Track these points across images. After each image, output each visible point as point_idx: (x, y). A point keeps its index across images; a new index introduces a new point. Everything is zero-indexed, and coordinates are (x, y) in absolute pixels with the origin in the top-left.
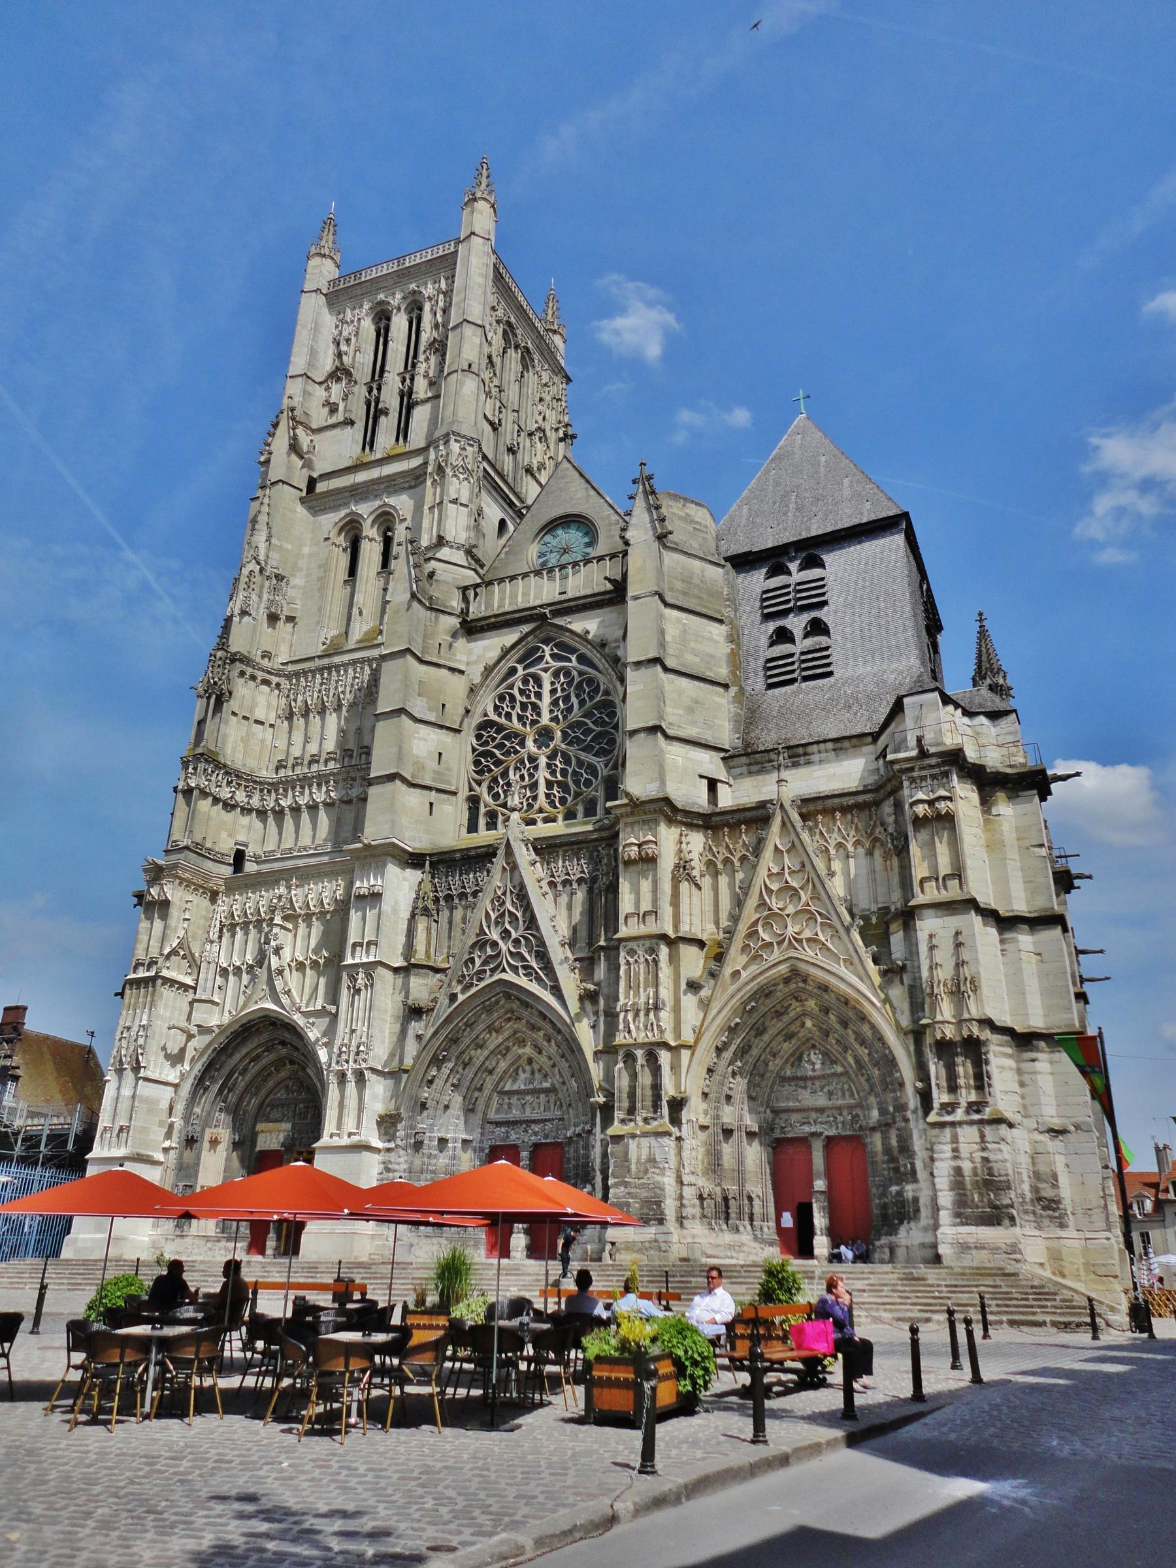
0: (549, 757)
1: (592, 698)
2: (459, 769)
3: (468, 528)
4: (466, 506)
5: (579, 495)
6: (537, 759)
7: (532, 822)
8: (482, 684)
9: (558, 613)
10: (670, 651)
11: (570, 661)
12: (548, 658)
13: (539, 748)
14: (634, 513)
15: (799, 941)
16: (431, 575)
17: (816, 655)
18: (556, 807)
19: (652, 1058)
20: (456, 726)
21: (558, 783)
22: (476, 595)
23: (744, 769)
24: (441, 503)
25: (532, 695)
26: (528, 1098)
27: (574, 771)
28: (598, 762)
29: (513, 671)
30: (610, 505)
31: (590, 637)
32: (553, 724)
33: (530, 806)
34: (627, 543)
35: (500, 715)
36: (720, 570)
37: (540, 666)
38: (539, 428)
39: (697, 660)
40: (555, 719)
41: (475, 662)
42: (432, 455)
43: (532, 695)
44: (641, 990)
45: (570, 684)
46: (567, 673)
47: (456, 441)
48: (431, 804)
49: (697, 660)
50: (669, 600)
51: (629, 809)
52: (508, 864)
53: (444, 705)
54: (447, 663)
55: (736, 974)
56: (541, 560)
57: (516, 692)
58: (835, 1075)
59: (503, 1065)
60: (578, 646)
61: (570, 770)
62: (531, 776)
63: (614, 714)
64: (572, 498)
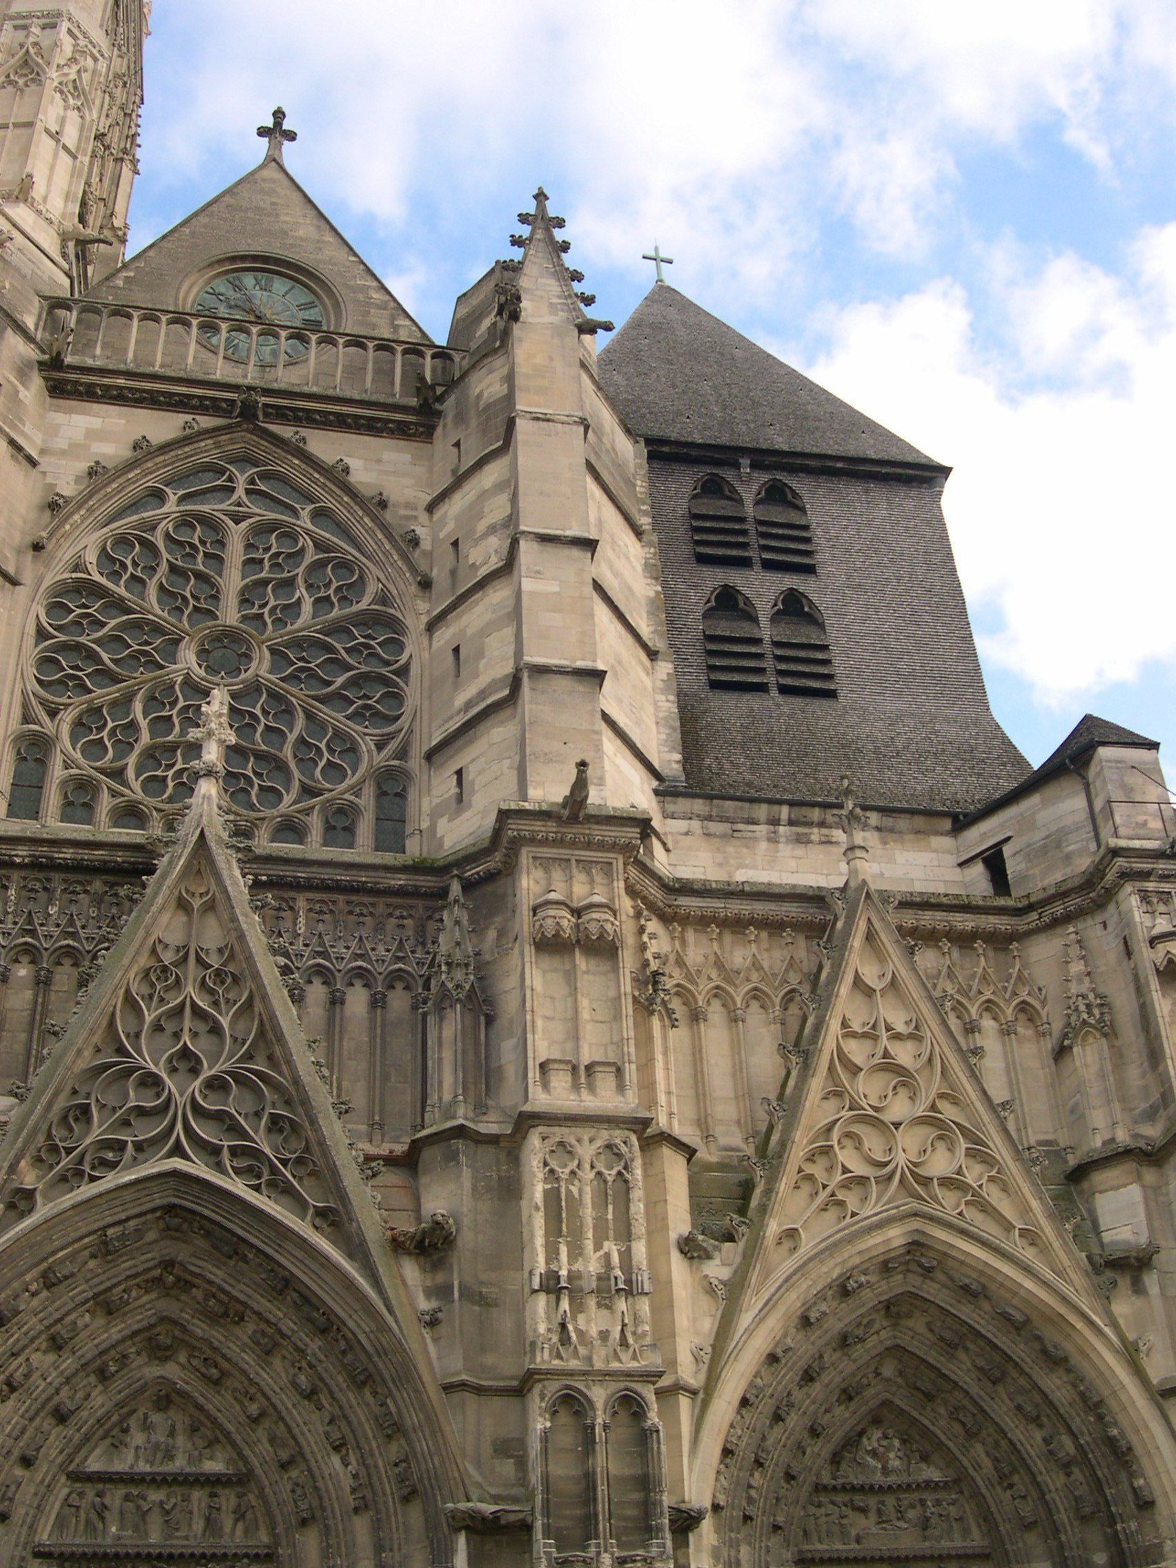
0: (234, 696)
9: (280, 414)
11: (295, 513)
12: (240, 492)
13: (210, 670)
15: (925, 1181)
17: (802, 654)
19: (630, 1406)
23: (695, 825)
26: (155, 1496)
27: (301, 741)
28: (365, 737)
29: (158, 496)
37: (223, 506)
41: (63, 453)
44: (589, 1245)
46: (290, 535)
51: (552, 826)
55: (792, 1234)
58: (929, 1485)
59: (100, 1401)
60: (318, 492)
61: (292, 737)
63: (401, 646)
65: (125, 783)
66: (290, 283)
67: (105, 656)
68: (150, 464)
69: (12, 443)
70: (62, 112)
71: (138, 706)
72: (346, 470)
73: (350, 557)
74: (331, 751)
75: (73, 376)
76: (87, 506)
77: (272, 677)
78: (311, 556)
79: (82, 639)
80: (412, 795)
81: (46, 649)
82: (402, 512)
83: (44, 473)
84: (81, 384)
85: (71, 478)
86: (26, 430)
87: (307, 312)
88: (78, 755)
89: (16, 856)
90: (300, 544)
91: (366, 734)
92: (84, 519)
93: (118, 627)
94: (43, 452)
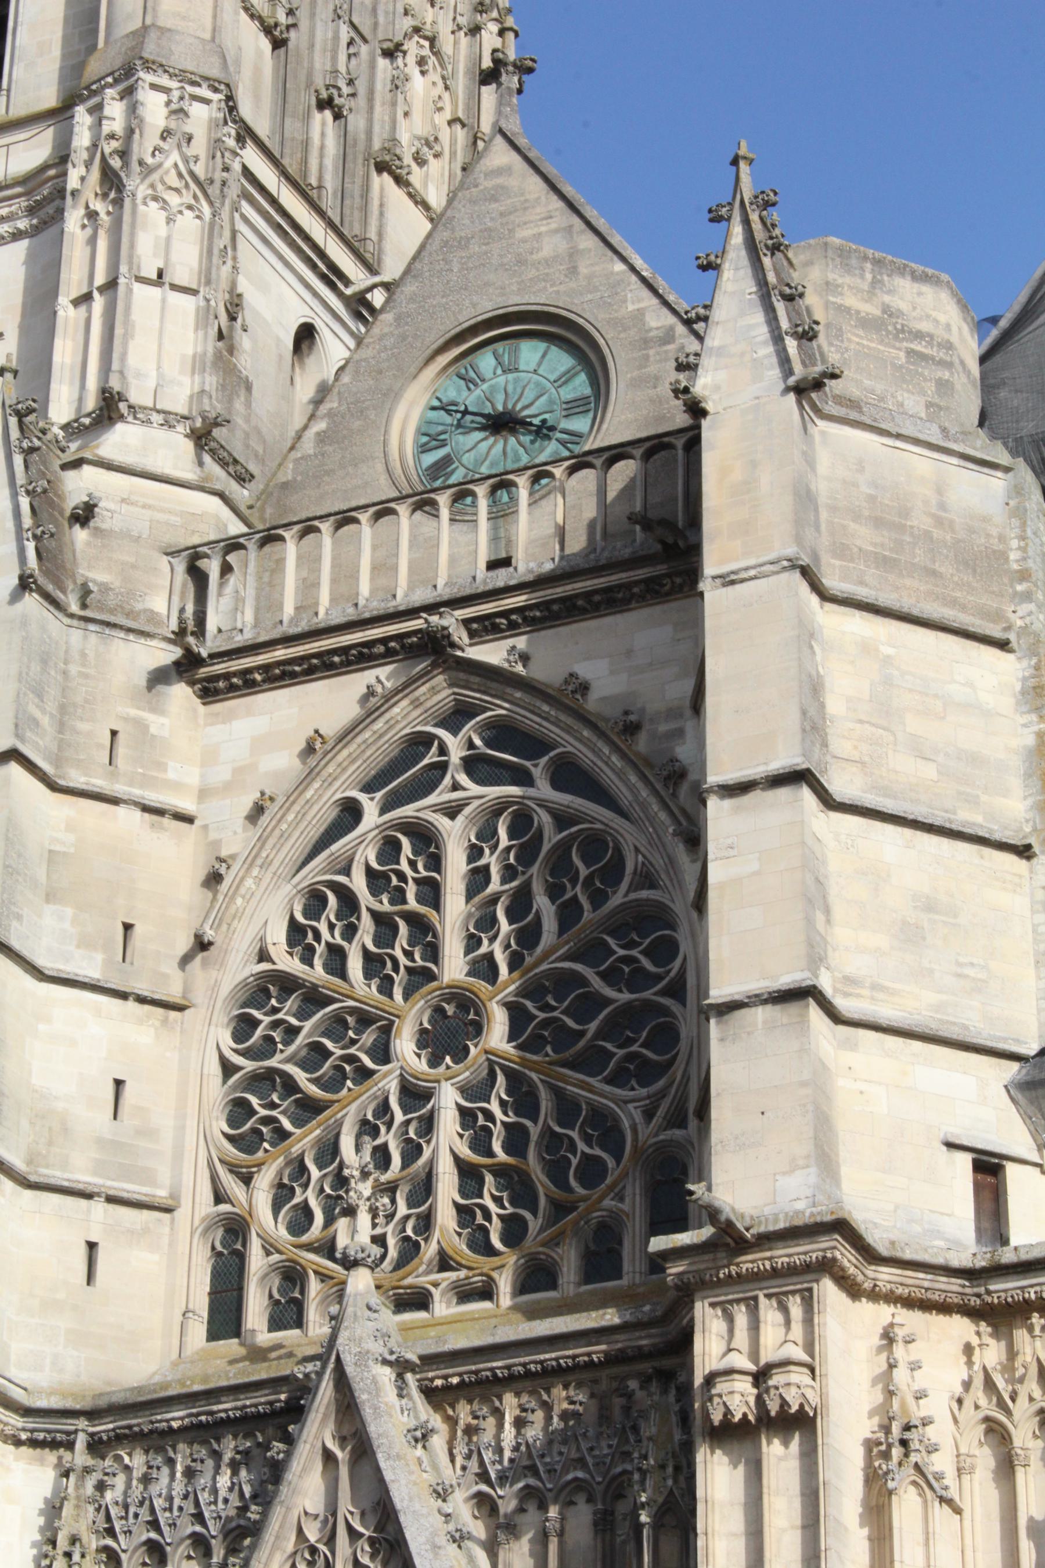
0: (464, 1090)
1: (598, 899)
2: (181, 1129)
3: (197, 365)
4: (194, 292)
5: (546, 251)
6: (426, 1095)
7: (419, 1300)
8: (250, 863)
10: (841, 744)
13: (435, 1061)
14: (718, 314)
16: (85, 515)
18: (491, 1251)
20: (173, 992)
21: (500, 1172)
22: (226, 569)
24: (111, 285)
27: (547, 1131)
30: (644, 280)
31: (592, 703)
32: (481, 986)
33: (410, 1250)
34: (697, 410)
35: (307, 959)
36: (997, 483)
37: (432, 799)
38: (417, 30)
39: (929, 772)
40: (485, 968)
41: (228, 788)
42: (82, 139)
45: (527, 853)
47: (154, 87)
48: (92, 1246)
49: (929, 772)
50: (832, 582)
52: (342, 1441)
53: (128, 927)
54: (137, 792)
56: (429, 459)
57: (358, 883)
60: (553, 732)
61: (534, 1131)
62: (412, 1151)
64: (521, 262)
66: (542, 346)
68: (330, 769)
69: (146, 809)
70: (163, 230)
73: (598, 826)
74: (588, 1140)
75: (219, 668)
76: (259, 862)
78: (551, 838)
79: (273, 1062)
81: (234, 1088)
82: (663, 728)
83: (205, 827)
84: (235, 674)
86: (171, 775)
87: (570, 386)
89: (173, 1419)
90: (536, 824)
91: (626, 1102)
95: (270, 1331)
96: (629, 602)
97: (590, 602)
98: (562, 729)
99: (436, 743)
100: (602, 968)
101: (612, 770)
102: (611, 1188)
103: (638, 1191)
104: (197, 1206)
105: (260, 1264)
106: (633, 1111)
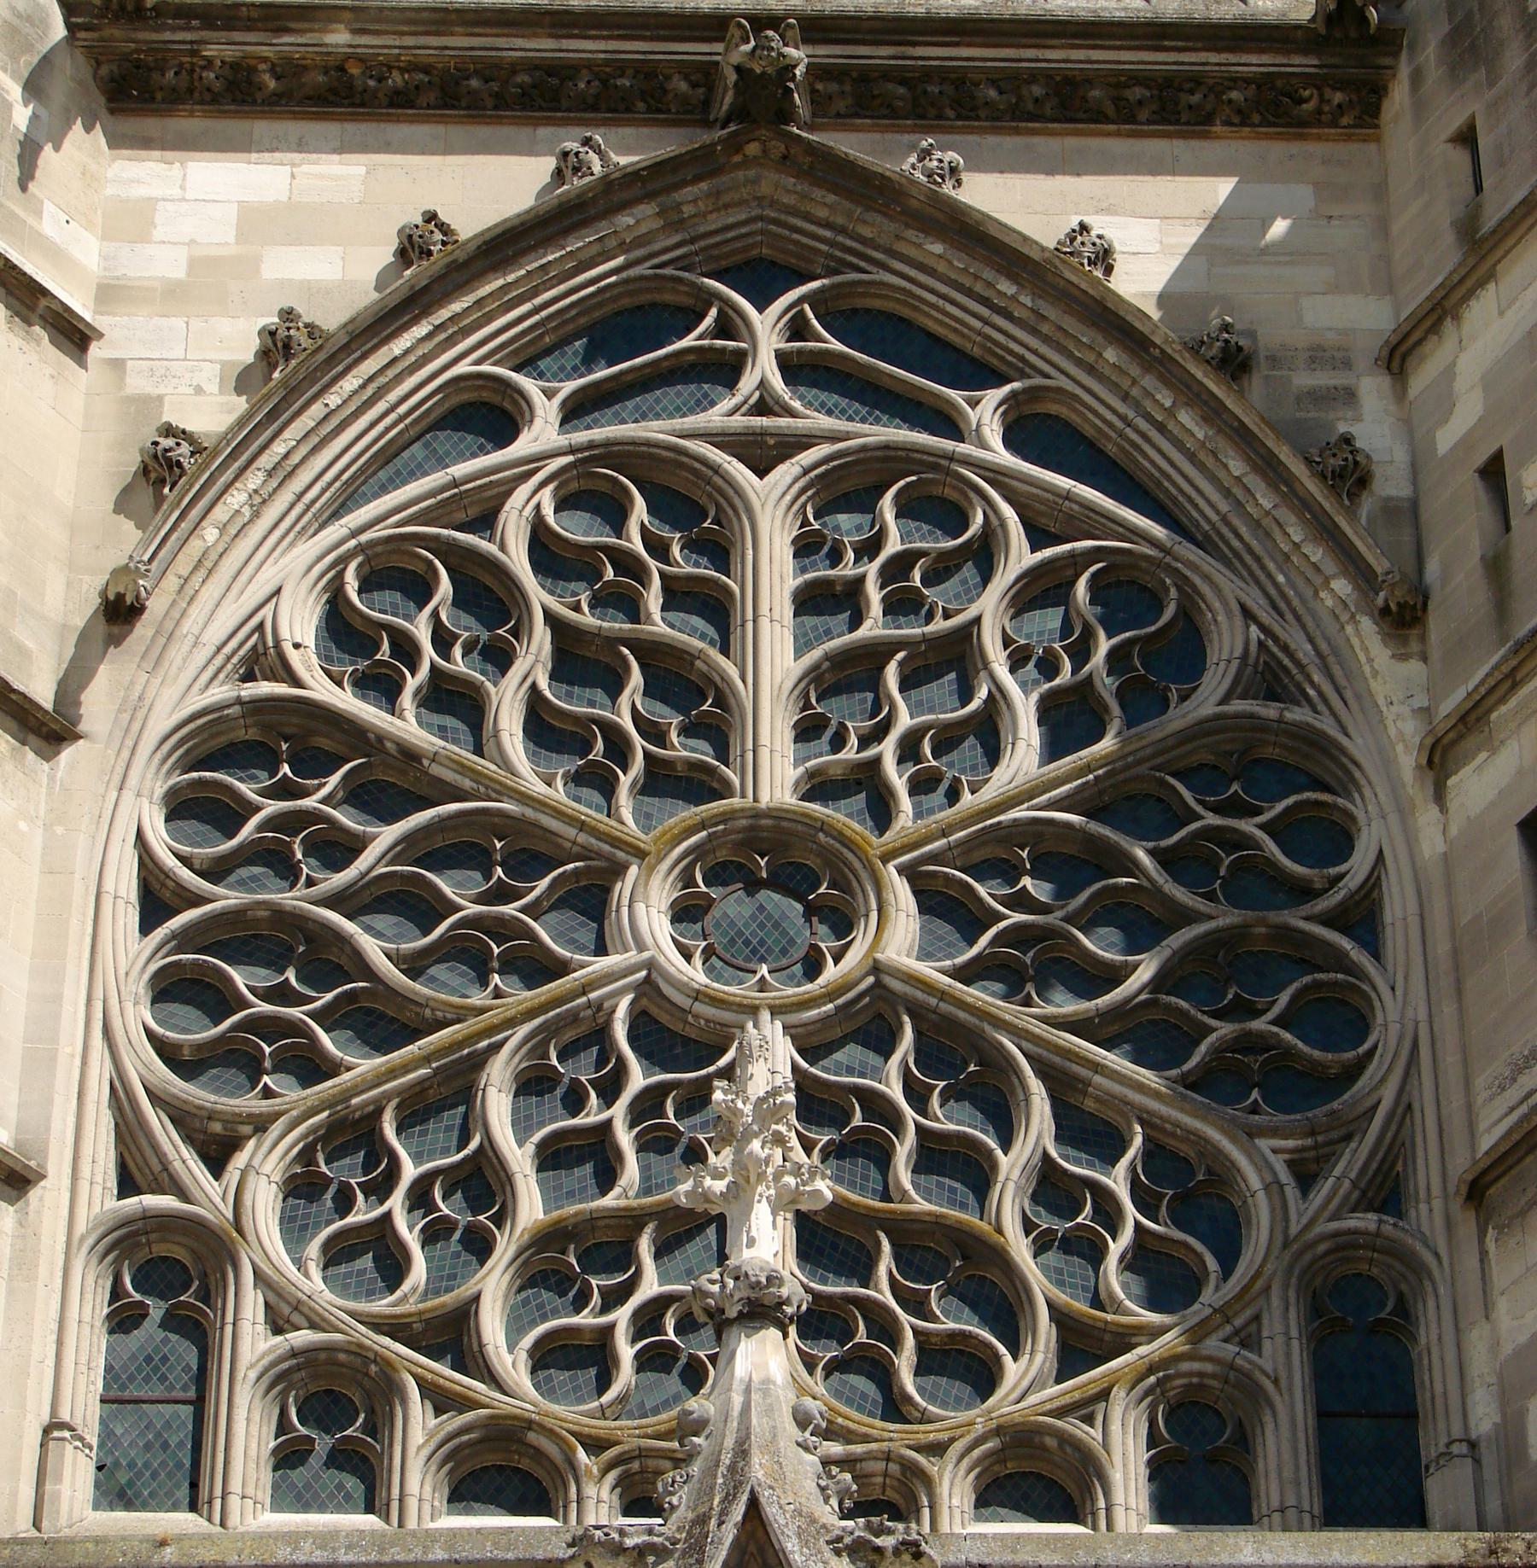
0: (812, 1045)
11: (948, 424)
12: (764, 368)
25: (653, 599)
37: (718, 416)
41: (172, 296)
43: (653, 599)
60: (1020, 341)
65: (470, 1358)
67: (373, 948)
71: (498, 1105)
72: (1104, 257)
76: (266, 461)
77: (926, 969)
78: (1019, 557)
79: (291, 898)
80: (1432, 1329)
81: (183, 940)
82: (1304, 380)
83: (118, 365)
85: (209, 378)
88: (313, 1284)
92: (258, 504)
93: (406, 848)
94: (109, 293)
95: (277, 1506)
96: (1208, 120)
97: (1116, 100)
98: (1046, 339)
99: (713, 312)
100: (1165, 843)
101: (1179, 444)
102: (1224, 1313)
103: (1294, 1333)
104: (84, 1186)
105: (263, 1346)
106: (1272, 1157)
